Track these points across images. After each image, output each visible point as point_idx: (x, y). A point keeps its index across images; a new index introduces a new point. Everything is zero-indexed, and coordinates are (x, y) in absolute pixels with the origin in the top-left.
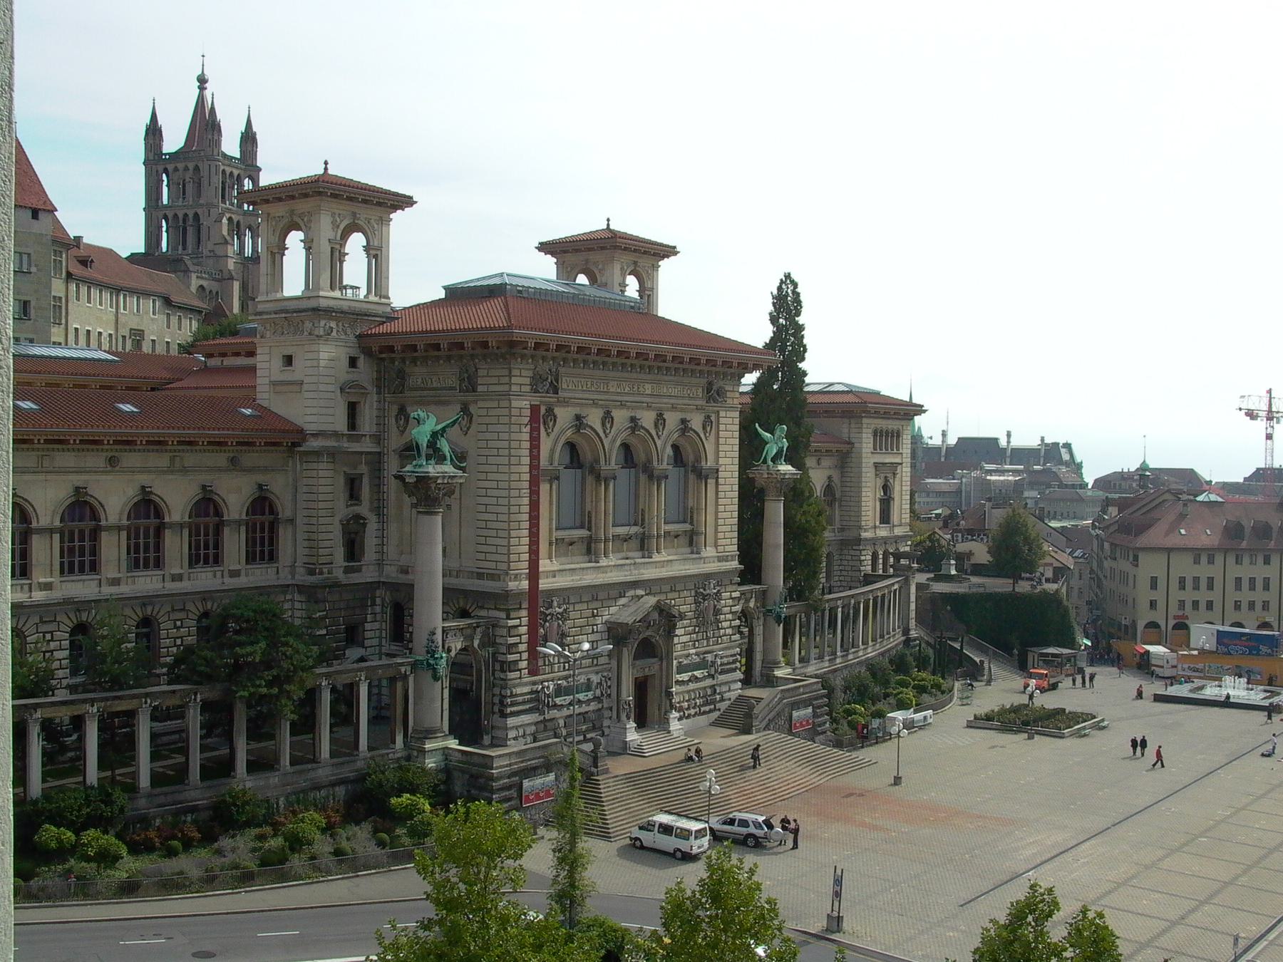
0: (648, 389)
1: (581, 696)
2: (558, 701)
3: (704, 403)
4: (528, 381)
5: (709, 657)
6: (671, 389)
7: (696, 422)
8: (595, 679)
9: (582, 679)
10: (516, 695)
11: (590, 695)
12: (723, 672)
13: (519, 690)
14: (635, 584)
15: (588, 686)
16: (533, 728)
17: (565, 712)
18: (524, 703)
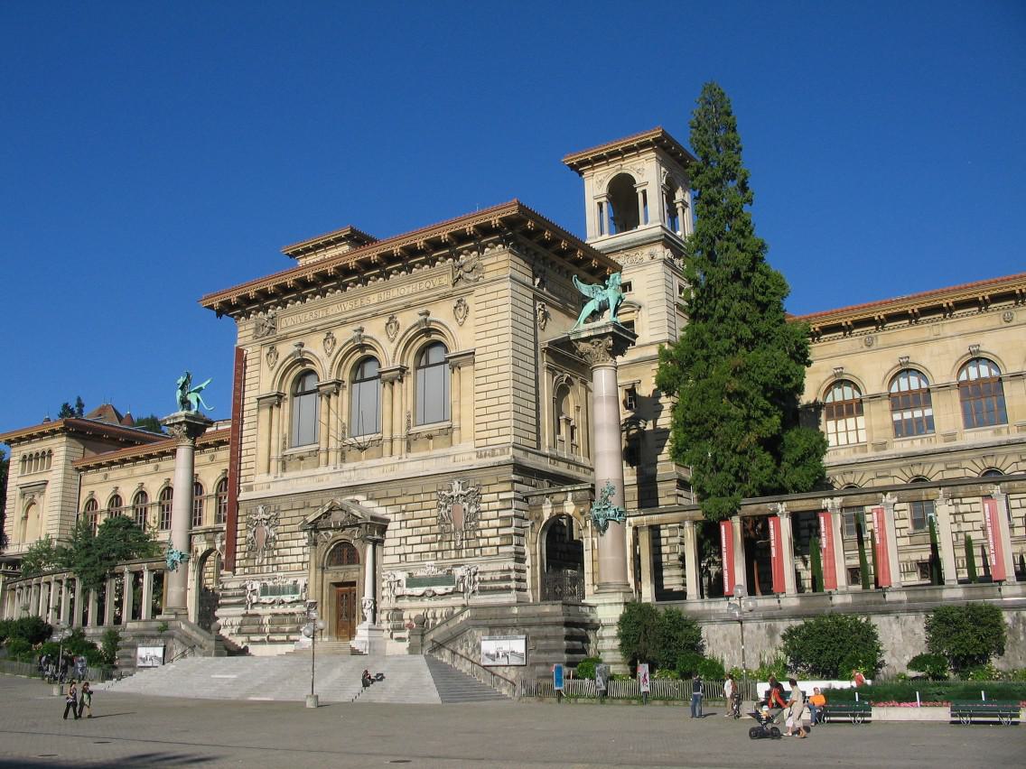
0: (374, 298)
1: (287, 598)
2: (265, 599)
3: (451, 288)
4: (251, 332)
5: (459, 572)
6: (401, 288)
7: (442, 314)
8: (301, 582)
9: (290, 582)
10: (227, 589)
11: (297, 597)
12: (483, 591)
13: (229, 586)
14: (354, 489)
15: (295, 590)
16: (239, 620)
17: (269, 610)
18: (233, 596)
